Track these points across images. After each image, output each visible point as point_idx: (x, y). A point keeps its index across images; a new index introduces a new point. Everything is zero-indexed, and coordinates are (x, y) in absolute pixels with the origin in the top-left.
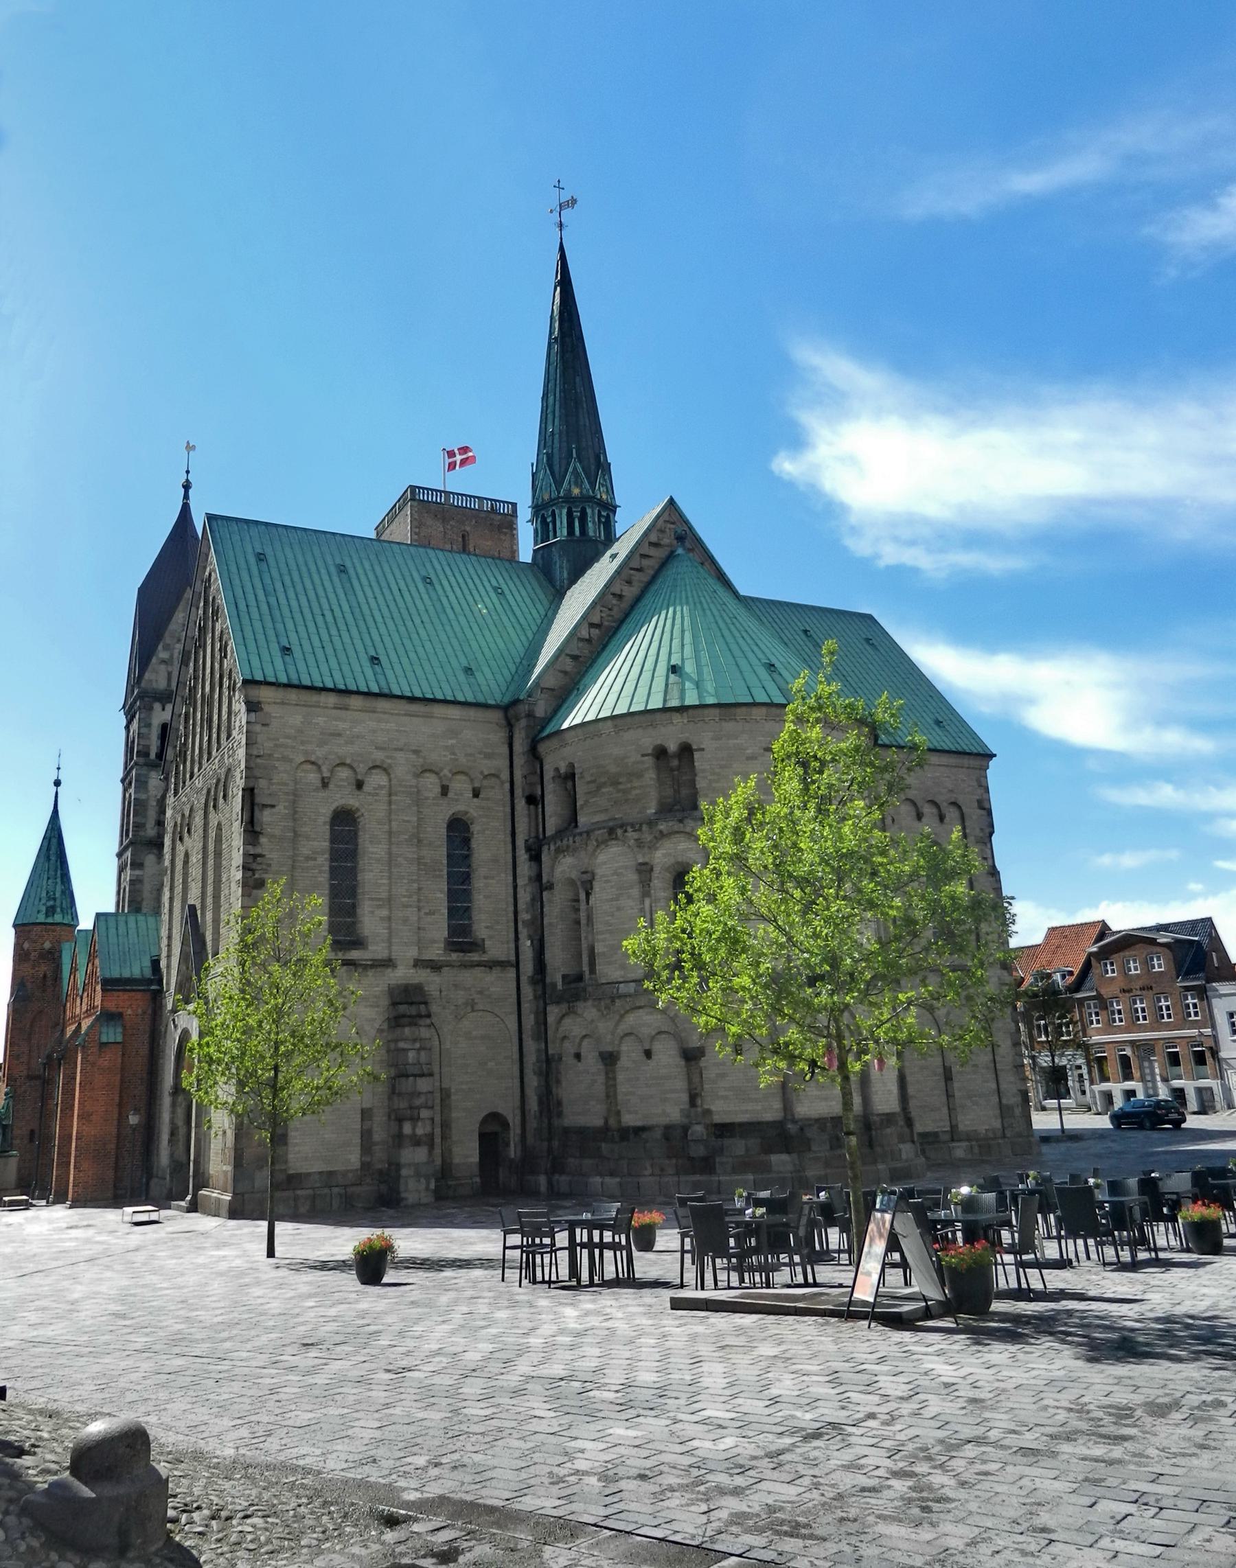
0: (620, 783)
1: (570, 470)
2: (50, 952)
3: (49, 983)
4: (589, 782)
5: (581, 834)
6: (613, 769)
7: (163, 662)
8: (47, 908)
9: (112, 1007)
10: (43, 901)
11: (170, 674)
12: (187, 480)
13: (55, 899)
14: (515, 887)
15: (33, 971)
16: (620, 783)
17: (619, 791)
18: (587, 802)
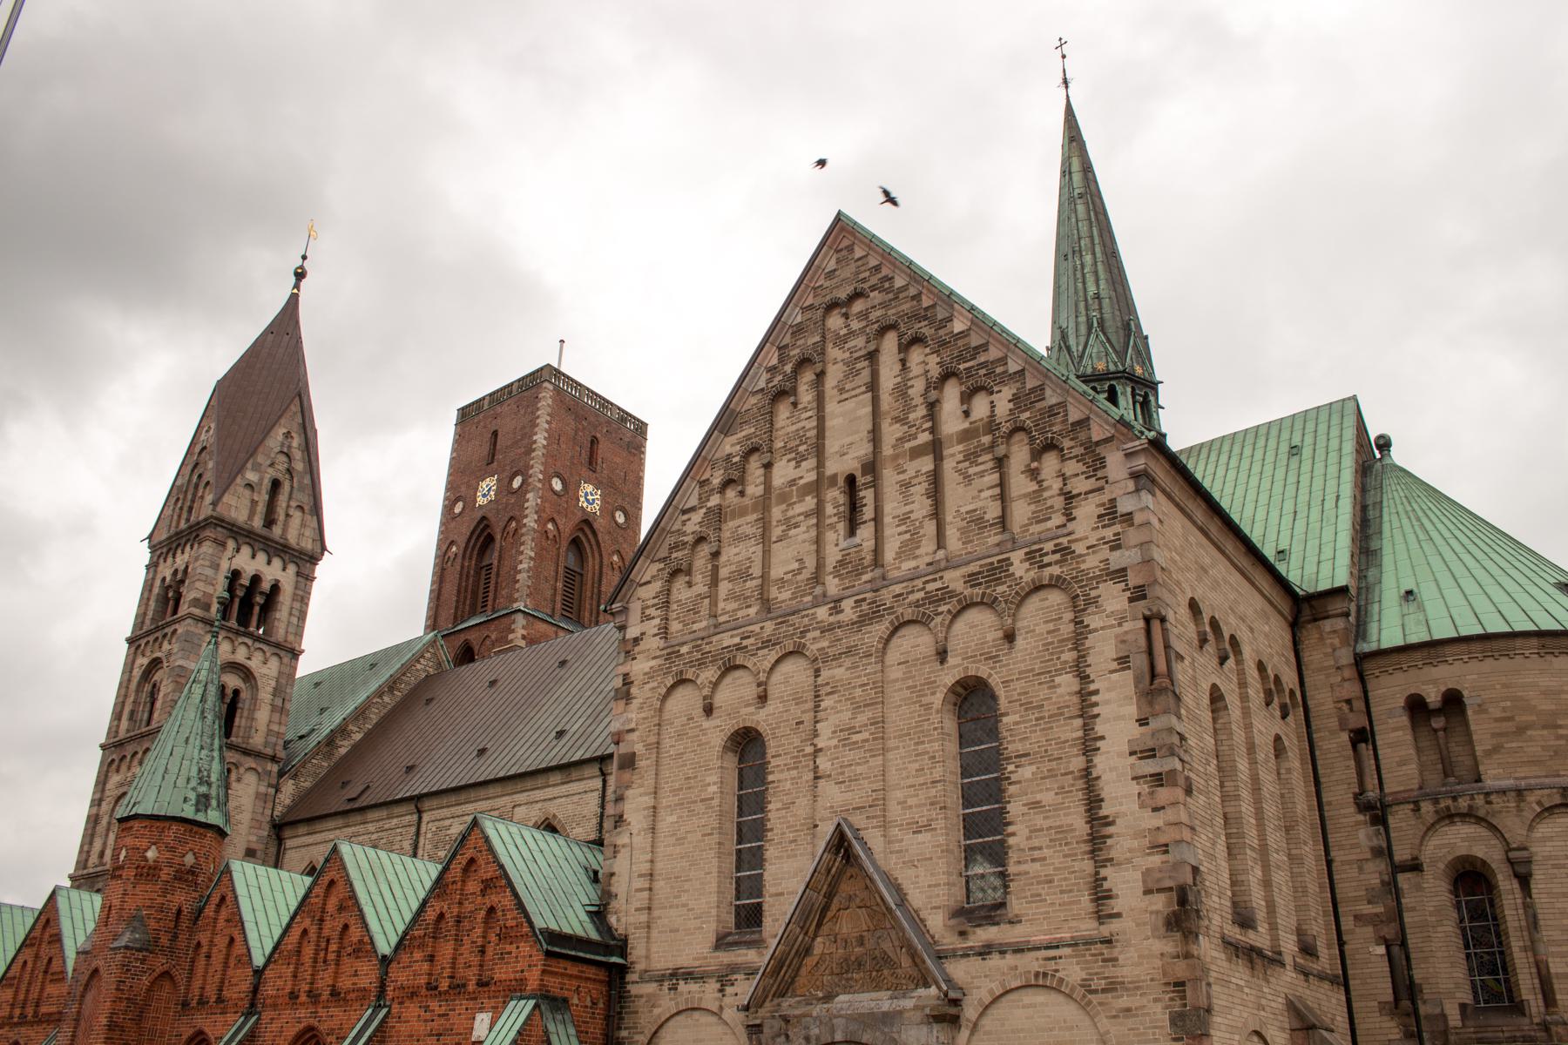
0: (1560, 727)
1: (1131, 343)
2: (192, 872)
3: (184, 924)
4: (1497, 720)
5: (1503, 792)
6: (1546, 706)
7: (249, 486)
8: (199, 796)
9: (553, 983)
10: (193, 783)
11: (254, 503)
12: (301, 267)
13: (209, 785)
14: (1329, 863)
15: (160, 900)
16: (1560, 727)
17: (1559, 737)
18: (1496, 749)
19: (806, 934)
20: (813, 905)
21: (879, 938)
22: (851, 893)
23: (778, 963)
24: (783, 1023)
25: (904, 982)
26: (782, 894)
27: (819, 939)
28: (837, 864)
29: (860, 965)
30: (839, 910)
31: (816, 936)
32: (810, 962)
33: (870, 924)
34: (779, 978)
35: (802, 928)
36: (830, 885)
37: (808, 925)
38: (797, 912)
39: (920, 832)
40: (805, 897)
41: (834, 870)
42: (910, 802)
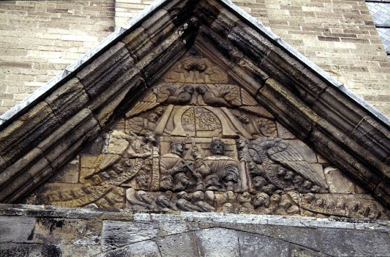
19: (96, 112)
20: (121, 73)
21: (268, 147)
22: (195, 86)
23: (29, 133)
24: (41, 230)
25: (343, 212)
26: (27, 66)
27: (115, 133)
28: (174, 37)
29: (223, 180)
30: (165, 103)
31: (108, 127)
32: (89, 163)
33: (243, 132)
34: (18, 165)
35: (91, 99)
36: (155, 60)
37: (105, 97)
38: (93, 67)
39: (337, 39)
40: (113, 51)
41: (168, 42)
42: (305, 9)
